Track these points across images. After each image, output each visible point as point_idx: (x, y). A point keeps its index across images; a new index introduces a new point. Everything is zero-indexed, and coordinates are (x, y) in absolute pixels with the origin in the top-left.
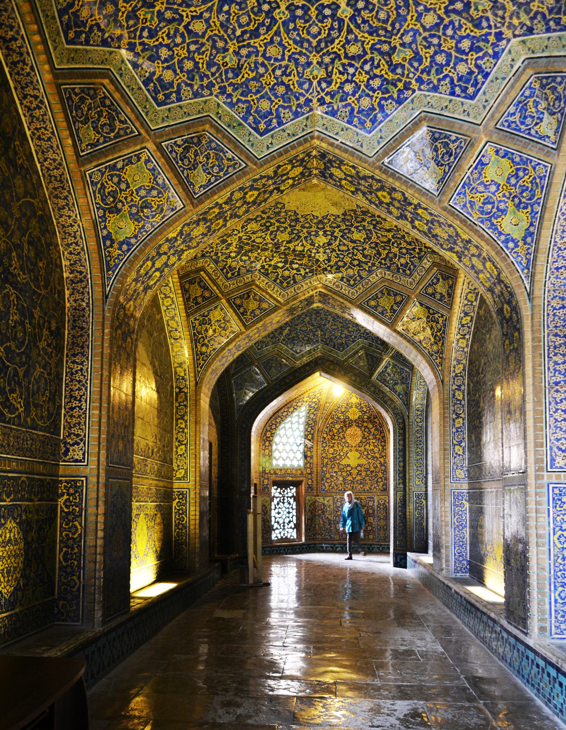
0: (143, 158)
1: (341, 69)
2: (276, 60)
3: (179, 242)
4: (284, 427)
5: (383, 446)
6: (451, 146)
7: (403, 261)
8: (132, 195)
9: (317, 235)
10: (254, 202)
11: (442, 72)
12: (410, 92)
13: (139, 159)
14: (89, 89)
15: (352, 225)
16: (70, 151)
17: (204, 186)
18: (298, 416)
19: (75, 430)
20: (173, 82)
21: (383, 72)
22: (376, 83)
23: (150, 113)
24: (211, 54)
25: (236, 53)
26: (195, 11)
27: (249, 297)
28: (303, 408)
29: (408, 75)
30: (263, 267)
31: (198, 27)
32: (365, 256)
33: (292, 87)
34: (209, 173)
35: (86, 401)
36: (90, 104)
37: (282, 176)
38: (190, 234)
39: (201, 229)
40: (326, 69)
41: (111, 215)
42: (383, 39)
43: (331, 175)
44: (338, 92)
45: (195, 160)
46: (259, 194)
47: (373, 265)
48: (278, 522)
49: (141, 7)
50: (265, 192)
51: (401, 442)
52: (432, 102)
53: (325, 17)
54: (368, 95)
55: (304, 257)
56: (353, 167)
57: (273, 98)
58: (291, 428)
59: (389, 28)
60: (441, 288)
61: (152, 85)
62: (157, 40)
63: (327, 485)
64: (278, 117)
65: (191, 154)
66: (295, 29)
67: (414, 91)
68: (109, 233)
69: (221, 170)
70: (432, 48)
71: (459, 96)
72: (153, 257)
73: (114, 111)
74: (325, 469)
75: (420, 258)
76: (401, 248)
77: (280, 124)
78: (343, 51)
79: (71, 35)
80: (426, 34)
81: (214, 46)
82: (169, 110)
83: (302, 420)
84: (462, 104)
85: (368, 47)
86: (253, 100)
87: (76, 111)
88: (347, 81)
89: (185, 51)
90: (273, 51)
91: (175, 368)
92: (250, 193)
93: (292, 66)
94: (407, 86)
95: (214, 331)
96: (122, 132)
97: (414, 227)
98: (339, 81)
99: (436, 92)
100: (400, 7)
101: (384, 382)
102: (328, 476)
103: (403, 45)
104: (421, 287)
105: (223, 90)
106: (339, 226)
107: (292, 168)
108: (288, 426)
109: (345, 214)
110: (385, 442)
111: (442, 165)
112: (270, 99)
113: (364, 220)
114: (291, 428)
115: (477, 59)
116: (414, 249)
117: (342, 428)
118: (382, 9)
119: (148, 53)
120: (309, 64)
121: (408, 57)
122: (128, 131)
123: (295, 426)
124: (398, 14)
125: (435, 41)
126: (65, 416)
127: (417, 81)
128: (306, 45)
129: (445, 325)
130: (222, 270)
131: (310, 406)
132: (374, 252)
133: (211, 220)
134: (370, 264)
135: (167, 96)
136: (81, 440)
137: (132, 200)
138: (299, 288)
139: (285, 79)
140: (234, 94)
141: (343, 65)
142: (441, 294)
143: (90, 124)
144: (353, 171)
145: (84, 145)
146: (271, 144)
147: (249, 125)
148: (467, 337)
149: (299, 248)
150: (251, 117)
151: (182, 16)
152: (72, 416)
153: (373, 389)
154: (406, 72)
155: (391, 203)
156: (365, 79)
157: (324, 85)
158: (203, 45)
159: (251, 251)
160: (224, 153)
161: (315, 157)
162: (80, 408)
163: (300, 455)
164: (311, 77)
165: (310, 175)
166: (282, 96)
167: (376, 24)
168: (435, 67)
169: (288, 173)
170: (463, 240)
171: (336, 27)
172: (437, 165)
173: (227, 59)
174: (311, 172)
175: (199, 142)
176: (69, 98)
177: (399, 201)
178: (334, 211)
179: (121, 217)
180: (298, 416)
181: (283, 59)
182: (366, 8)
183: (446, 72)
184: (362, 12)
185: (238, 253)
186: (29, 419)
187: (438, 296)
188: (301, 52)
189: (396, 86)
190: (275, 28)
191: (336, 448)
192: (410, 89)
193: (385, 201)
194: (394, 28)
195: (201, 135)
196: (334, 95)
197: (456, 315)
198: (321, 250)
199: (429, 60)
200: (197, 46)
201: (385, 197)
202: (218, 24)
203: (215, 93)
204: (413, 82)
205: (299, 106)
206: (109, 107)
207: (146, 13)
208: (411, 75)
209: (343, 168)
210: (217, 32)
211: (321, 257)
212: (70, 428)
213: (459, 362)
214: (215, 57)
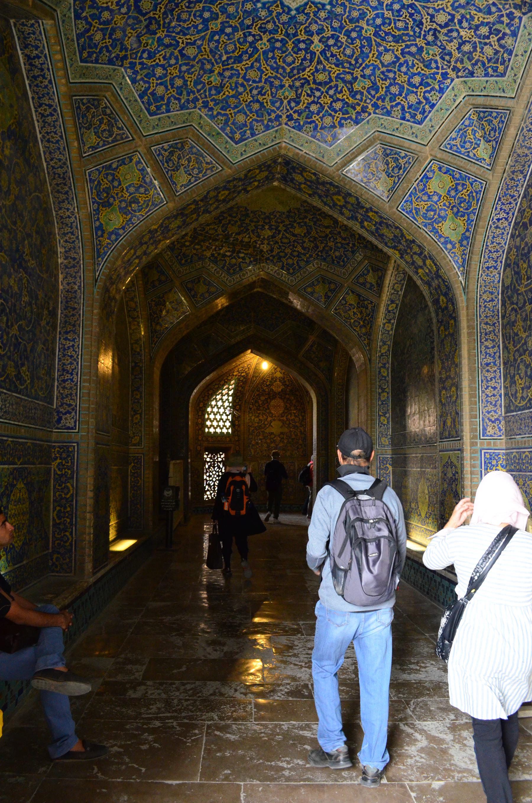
0: (135, 160)
1: (309, 92)
2: (254, 81)
3: (159, 233)
4: (216, 399)
5: (303, 416)
6: (401, 161)
7: (337, 254)
8: (122, 191)
9: (263, 228)
10: (224, 200)
11: (395, 100)
12: (367, 114)
13: (131, 160)
14: (94, 100)
15: (295, 221)
16: (74, 154)
17: (185, 186)
18: (228, 388)
19: (67, 401)
20: (164, 95)
21: (345, 97)
22: (338, 105)
23: (143, 122)
24: (199, 74)
25: (220, 74)
26: (190, 39)
27: (199, 281)
28: (232, 382)
29: (366, 100)
30: (213, 255)
31: (191, 52)
32: (304, 248)
33: (265, 104)
34: (190, 174)
35: (77, 374)
36: (94, 112)
37: (251, 179)
38: (168, 226)
39: (178, 222)
40: (296, 91)
41: (104, 209)
42: (347, 70)
43: (292, 180)
44: (305, 111)
45: (178, 163)
46: (229, 194)
47: (311, 256)
49: (145, 34)
50: (234, 192)
52: (385, 124)
53: (300, 50)
54: (330, 115)
55: (250, 247)
56: (315, 174)
57: (248, 113)
59: (353, 62)
60: (371, 278)
61: (146, 97)
62: (154, 61)
64: (252, 128)
65: (175, 158)
66: (273, 58)
67: (370, 114)
68: (101, 224)
69: (200, 172)
70: (388, 81)
71: (408, 121)
72: (136, 246)
73: (113, 119)
74: (251, 437)
75: (353, 252)
76: (337, 243)
77: (253, 135)
78: (312, 78)
79: (85, 55)
80: (384, 69)
81: (202, 68)
82: (159, 119)
83: (231, 393)
84: (411, 127)
85: (333, 76)
86: (231, 114)
87: (83, 119)
88: (313, 102)
89: (177, 71)
90: (252, 74)
91: (132, 344)
92: (223, 192)
93: (267, 87)
94: (364, 110)
95: (168, 312)
96: (118, 137)
97: (363, 227)
98: (306, 101)
99: (389, 116)
100: (365, 46)
102: (253, 442)
103: (363, 76)
104: (353, 277)
105: (205, 105)
106: (283, 222)
107: (260, 172)
108: (218, 397)
109: (290, 211)
110: (305, 412)
111: (392, 176)
112: (245, 113)
113: (306, 217)
114: (222, 399)
115: (424, 93)
116: (348, 244)
117: (266, 399)
118: (349, 47)
119: (145, 72)
120: (282, 86)
121: (367, 86)
122: (124, 136)
123: (225, 398)
124: (362, 52)
125: (391, 75)
126: (58, 387)
127: (373, 106)
128: (281, 71)
129: (373, 311)
130: (177, 257)
131: (239, 380)
132: (312, 245)
133: (187, 214)
134: (308, 255)
135: (158, 108)
136: (73, 409)
137: (122, 196)
138: (244, 275)
139: (260, 98)
140: (215, 108)
141: (311, 89)
142: (371, 283)
143: (92, 129)
144: (313, 177)
145: (86, 147)
146: (245, 151)
147: (226, 134)
148: (392, 321)
149: (246, 240)
150: (228, 128)
151: (178, 42)
152: (64, 388)
154: (364, 98)
155: (344, 206)
156: (329, 102)
157: (293, 104)
158: (193, 66)
159: (204, 241)
160: (203, 158)
161: (280, 163)
162: (72, 380)
163: (228, 424)
164: (283, 97)
165: (273, 179)
166: (257, 112)
167: (343, 58)
168: (389, 96)
169: (255, 176)
170: (407, 240)
171: (309, 58)
172: (388, 176)
173: (212, 79)
174: (274, 176)
175: (183, 147)
176: (79, 108)
177: (352, 205)
178: (280, 208)
179: (112, 210)
180: (228, 388)
181: (260, 81)
182: (335, 45)
183: (398, 101)
184: (332, 48)
185: (192, 242)
186: (33, 391)
187: (368, 286)
188: (276, 76)
189: (355, 109)
190: (256, 56)
191: (261, 418)
192: (367, 112)
193: (339, 203)
194: (357, 62)
195: (185, 142)
196: (301, 113)
197: (383, 302)
198: (266, 242)
199: (384, 89)
200: (187, 67)
201: (339, 200)
202: (208, 50)
203: (198, 107)
204: (370, 106)
205: (270, 120)
206: (109, 115)
207: (149, 38)
208: (368, 101)
209: (305, 174)
210: (206, 57)
211: (265, 248)
212: (63, 398)
213: (384, 343)
214: (202, 77)
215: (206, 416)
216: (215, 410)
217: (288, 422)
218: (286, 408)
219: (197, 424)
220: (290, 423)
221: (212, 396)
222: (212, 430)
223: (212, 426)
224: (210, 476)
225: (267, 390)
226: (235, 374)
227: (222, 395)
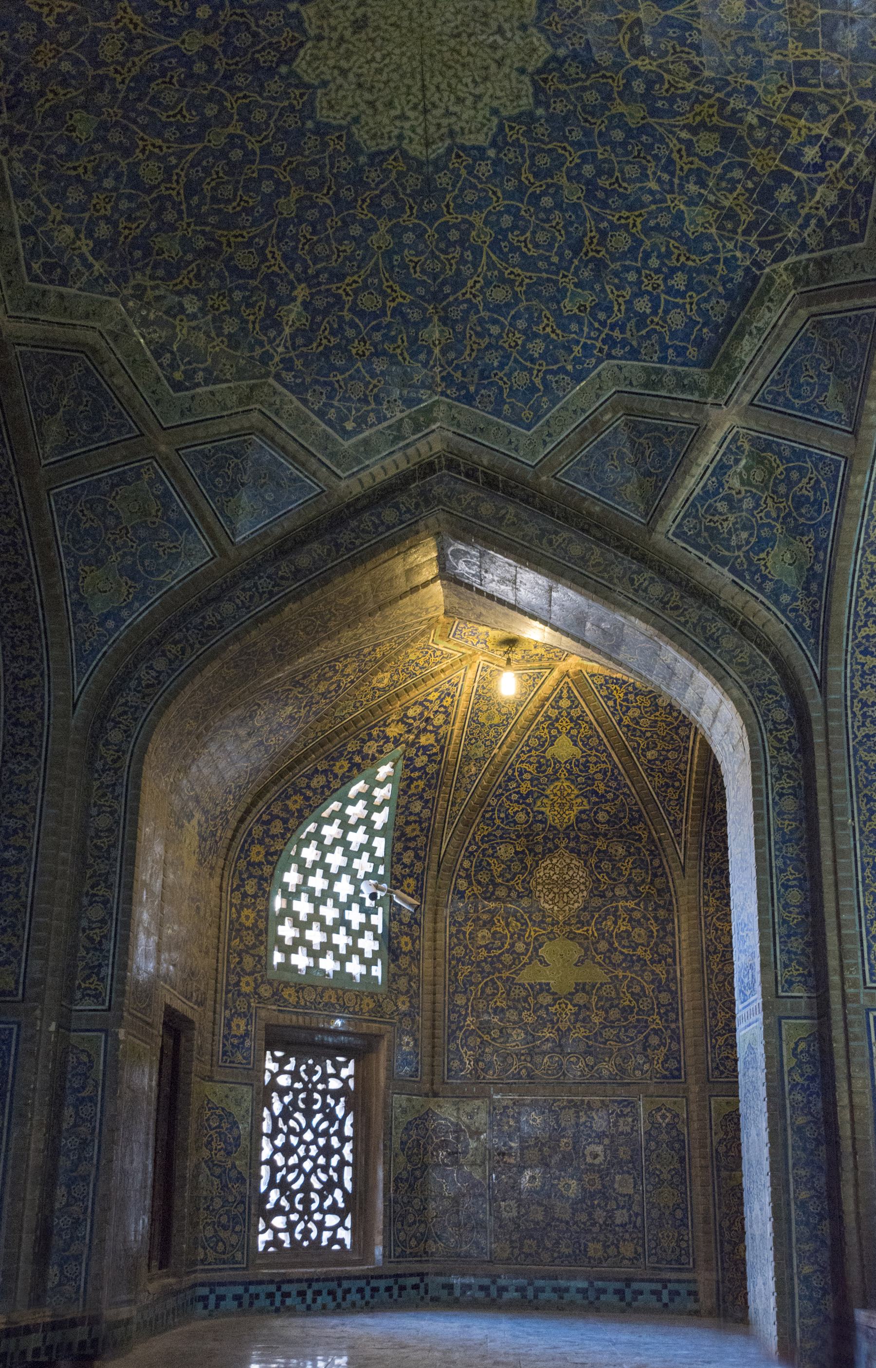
4: (318, 836)
5: (663, 924)
18: (368, 796)
28: (384, 771)
48: (284, 1187)
51: (789, 804)
58: (342, 842)
63: (468, 1056)
74: (460, 1000)
83: (380, 819)
101: (710, 540)
110: (668, 907)
114: (342, 842)
123: (357, 838)
131: (409, 762)
153: (657, 590)
163: (368, 944)
215: (279, 903)
216: (318, 882)
217: (603, 946)
218: (596, 892)
219: (237, 929)
220: (612, 949)
221: (302, 819)
222: (301, 960)
223: (300, 942)
224: (288, 1150)
225: (521, 817)
226: (393, 731)
227: (346, 827)
